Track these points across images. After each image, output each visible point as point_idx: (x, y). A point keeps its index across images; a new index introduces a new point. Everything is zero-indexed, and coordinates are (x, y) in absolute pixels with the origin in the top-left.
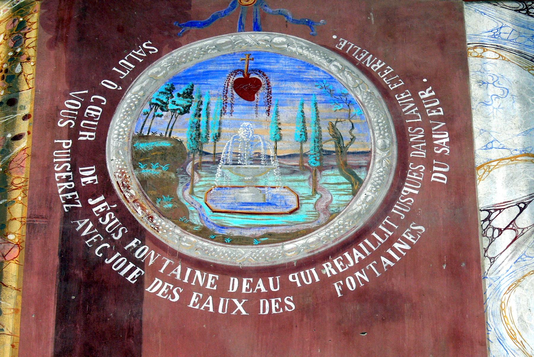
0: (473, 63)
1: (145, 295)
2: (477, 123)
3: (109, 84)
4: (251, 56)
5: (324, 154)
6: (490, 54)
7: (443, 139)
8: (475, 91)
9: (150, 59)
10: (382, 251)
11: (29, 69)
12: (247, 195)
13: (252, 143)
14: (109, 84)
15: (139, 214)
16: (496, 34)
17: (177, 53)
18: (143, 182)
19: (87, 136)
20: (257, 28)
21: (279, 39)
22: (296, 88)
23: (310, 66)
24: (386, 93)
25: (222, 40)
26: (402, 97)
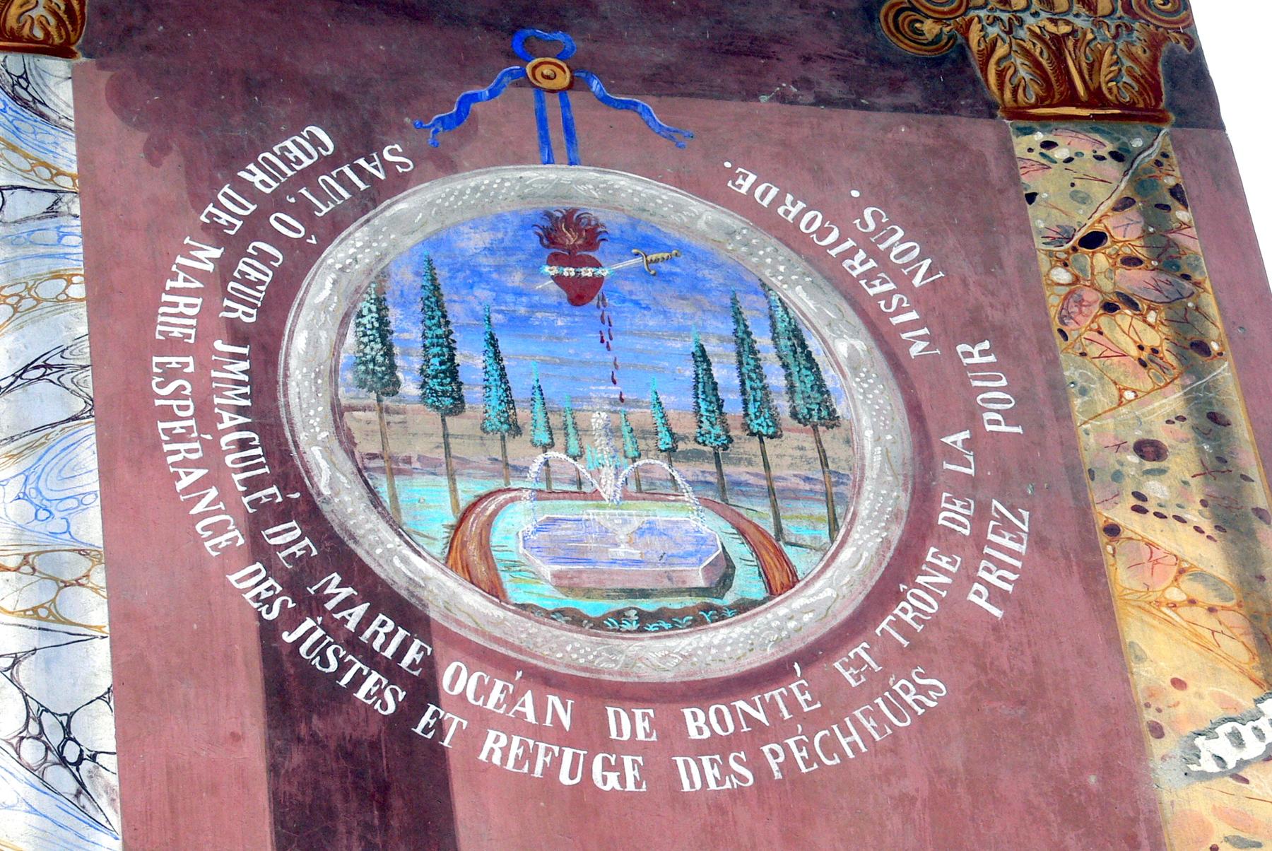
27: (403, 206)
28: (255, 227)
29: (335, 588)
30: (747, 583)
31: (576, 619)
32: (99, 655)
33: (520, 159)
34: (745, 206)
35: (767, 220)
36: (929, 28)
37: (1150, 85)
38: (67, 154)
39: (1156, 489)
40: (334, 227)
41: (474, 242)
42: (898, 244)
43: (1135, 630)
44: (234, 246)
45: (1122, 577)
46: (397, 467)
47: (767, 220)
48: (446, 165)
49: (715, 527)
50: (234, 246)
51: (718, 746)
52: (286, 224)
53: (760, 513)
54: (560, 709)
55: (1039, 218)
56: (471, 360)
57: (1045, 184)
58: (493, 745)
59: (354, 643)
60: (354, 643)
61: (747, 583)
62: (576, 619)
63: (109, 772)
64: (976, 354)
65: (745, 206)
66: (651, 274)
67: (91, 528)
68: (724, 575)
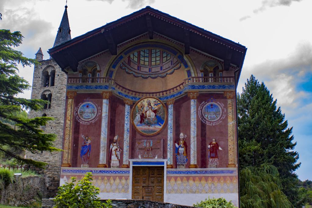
0: (103, 105)
1: (80, 124)
2: (103, 110)
3: (78, 106)
4: (88, 104)
5: (92, 112)
6: (104, 104)
7: (100, 111)
8: (103, 107)
9: (81, 104)
10: (95, 120)
11: (73, 105)
12: (87, 115)
13: (88, 111)
14: (78, 106)
15: (80, 117)
16: (105, 102)
17: (83, 104)
18: (80, 115)
19: (77, 111)
20: (88, 101)
21: (90, 102)
22: (91, 107)
23: (92, 105)
24: (97, 107)
25: (86, 102)
26: (98, 107)
27: (206, 104)
28: (202, 106)
29: (203, 119)
30: (216, 118)
31: (210, 120)
32: (196, 122)
33: (210, 102)
34: (218, 103)
35: (219, 104)
36: (225, 95)
37: (233, 97)
38: (196, 103)
39: (230, 114)
40: (204, 105)
41: (209, 106)
42: (223, 105)
43: (228, 119)
44: (201, 106)
45: (228, 117)
46: (205, 114)
47: (219, 104)
48: (208, 102)
49: (215, 116)
50: (201, 106)
51: (214, 124)
52: (203, 105)
53: (217, 115)
54: (210, 123)
55: (228, 103)
56: (208, 110)
57: (229, 102)
58: (208, 124)
59: (204, 121)
60: (204, 121)
61: (216, 118)
62: (210, 120)
63: (196, 125)
64: (225, 109)
65: (218, 103)
66: (214, 107)
67: (196, 117)
68: (215, 118)
